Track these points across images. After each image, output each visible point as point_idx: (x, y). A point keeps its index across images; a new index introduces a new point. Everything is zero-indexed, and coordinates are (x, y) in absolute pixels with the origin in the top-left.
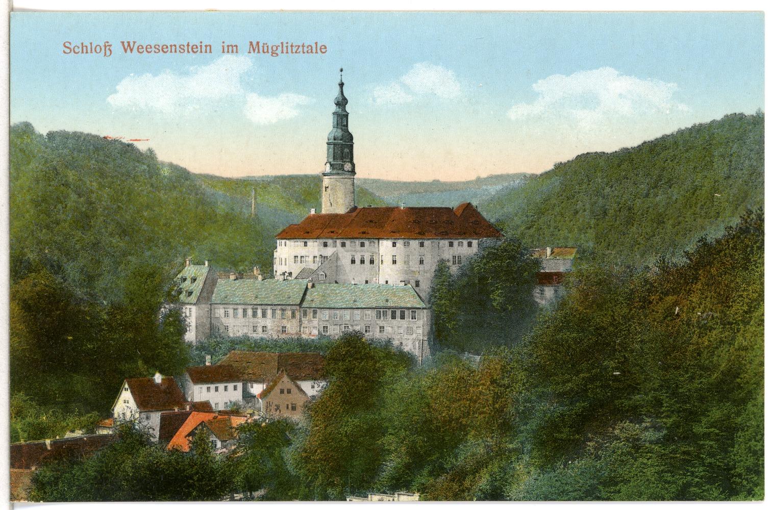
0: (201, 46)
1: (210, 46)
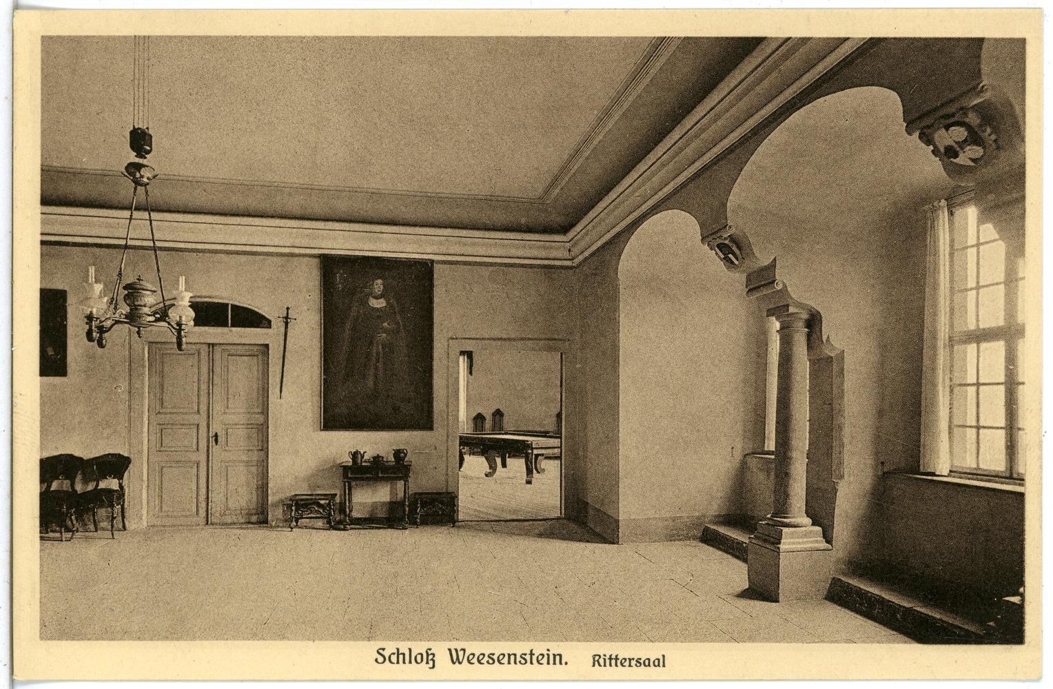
0: (548, 655)
1: (560, 655)
